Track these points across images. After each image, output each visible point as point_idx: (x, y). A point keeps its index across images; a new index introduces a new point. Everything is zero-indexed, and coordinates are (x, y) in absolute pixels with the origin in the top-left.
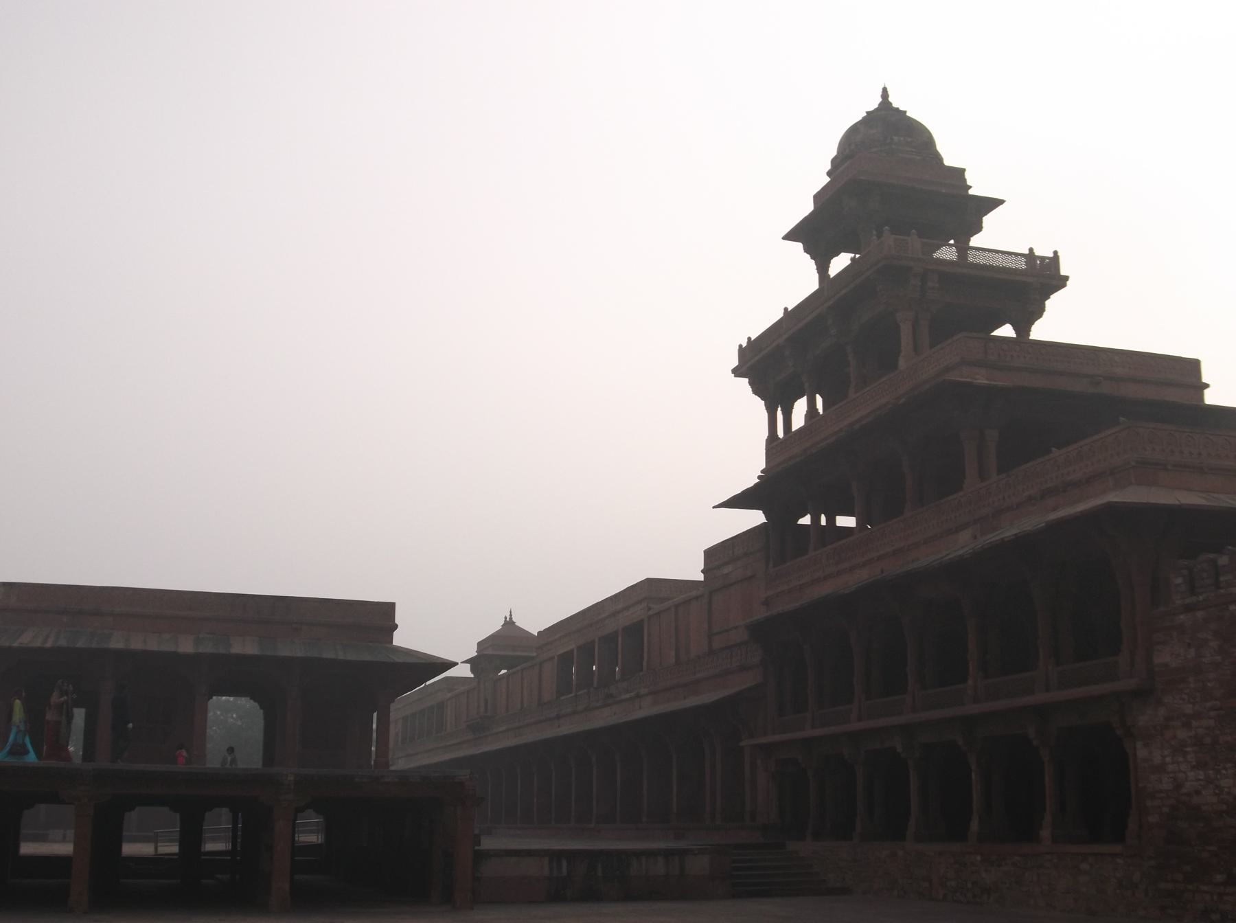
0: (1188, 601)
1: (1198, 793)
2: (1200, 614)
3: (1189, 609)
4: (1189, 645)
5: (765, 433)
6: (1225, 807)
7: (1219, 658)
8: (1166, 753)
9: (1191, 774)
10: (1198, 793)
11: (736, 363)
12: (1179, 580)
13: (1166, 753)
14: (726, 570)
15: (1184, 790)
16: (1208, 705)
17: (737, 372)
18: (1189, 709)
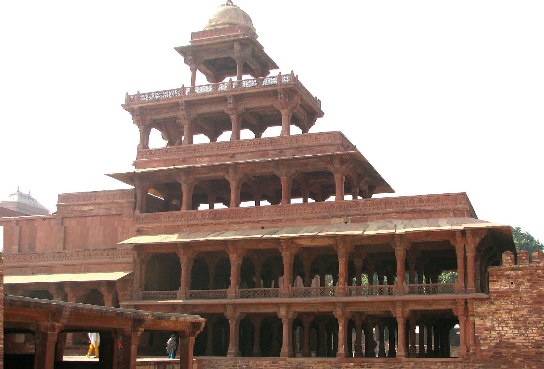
0: (512, 267)
1: (513, 338)
2: (519, 272)
3: (513, 269)
4: (512, 283)
5: (138, 142)
6: (530, 344)
7: (530, 290)
8: (494, 323)
9: (510, 332)
10: (513, 338)
11: (124, 102)
12: (509, 258)
13: (494, 323)
14: (86, 208)
15: (504, 337)
16: (523, 306)
17: (123, 106)
18: (511, 307)
